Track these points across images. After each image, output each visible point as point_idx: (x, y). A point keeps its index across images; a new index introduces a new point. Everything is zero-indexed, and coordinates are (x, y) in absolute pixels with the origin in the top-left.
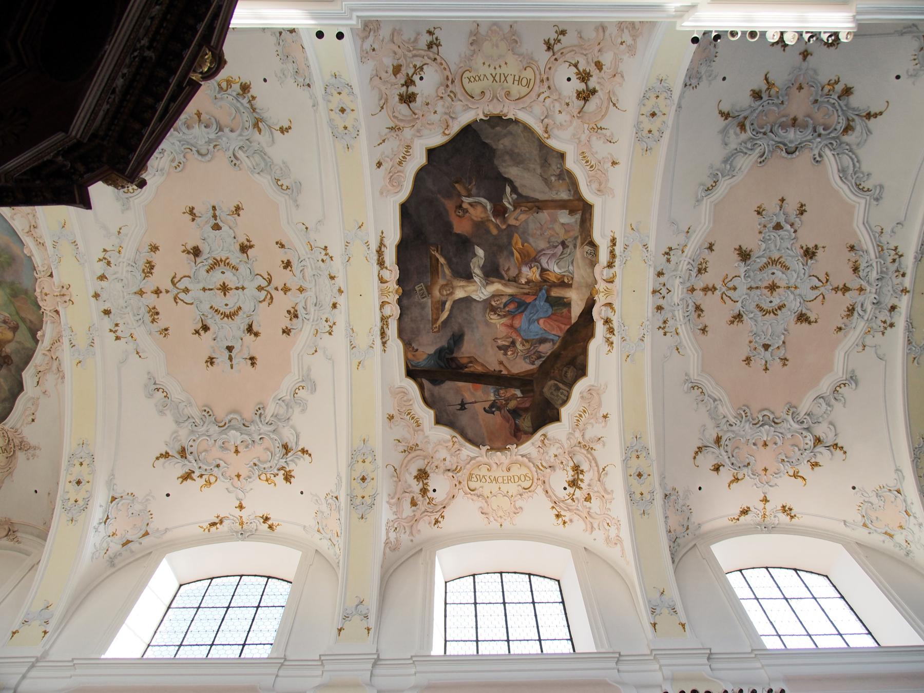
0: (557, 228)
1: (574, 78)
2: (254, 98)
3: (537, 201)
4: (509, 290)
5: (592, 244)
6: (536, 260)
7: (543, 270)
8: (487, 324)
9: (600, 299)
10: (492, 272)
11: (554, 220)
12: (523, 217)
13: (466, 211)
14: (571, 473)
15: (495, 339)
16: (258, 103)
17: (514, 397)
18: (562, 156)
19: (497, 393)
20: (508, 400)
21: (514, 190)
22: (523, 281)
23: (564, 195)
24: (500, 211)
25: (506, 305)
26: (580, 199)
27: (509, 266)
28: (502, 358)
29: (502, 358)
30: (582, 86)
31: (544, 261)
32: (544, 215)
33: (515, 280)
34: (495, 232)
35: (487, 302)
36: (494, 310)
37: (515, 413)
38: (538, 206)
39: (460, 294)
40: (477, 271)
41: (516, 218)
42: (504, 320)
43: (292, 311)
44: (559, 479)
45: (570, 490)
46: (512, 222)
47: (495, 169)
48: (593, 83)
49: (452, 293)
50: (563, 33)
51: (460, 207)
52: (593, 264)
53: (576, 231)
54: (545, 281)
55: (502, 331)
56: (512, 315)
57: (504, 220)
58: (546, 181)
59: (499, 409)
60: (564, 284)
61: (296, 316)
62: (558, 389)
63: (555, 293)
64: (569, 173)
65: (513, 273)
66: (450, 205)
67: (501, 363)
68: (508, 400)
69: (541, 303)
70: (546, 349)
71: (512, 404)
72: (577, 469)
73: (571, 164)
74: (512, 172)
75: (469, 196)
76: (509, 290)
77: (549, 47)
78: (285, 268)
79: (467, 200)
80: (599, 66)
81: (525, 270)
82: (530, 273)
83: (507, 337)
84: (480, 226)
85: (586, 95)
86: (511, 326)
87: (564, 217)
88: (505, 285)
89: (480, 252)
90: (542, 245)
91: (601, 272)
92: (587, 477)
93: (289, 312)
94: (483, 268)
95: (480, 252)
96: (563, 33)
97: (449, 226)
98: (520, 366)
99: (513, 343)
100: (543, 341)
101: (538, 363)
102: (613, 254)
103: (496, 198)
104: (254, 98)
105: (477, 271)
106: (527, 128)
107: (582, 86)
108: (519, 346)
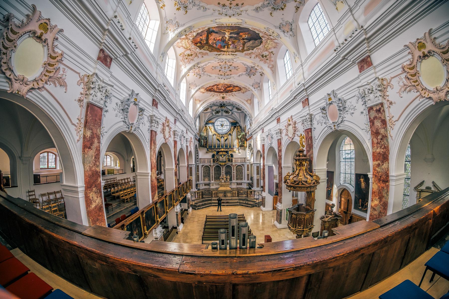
0: (239, 47)
1: (266, 55)
2: (280, 10)
3: (245, 45)
4: (227, 40)
5: (236, 52)
6: (233, 44)
7: (231, 45)
8: (219, 37)
9: (225, 53)
10: (231, 37)
11: (241, 47)
12: (242, 42)
13: (245, 35)
14: (190, 54)
15: (216, 38)
16: (278, 10)
17: (204, 42)
18: (253, 50)
19: (204, 39)
20: (203, 41)
21: (248, 42)
22: (229, 42)
23: (245, 49)
24: (243, 39)
25: (224, 39)
26: (244, 51)
27: (232, 40)
28: (212, 39)
29: (212, 39)
30: (264, 56)
31: (233, 45)
32: (242, 45)
33: (229, 40)
34: (239, 38)
35: (225, 36)
36: (223, 37)
37: (201, 43)
38: (244, 44)
39: (227, 33)
40: (231, 35)
41: (242, 41)
42: (220, 39)
43: (225, 5)
44: (188, 52)
45: (187, 55)
46: (241, 41)
47: (252, 40)
48: (265, 58)
49: (227, 32)
50: (273, 55)
51: (246, 34)
52: (232, 52)
53: (238, 49)
54: (229, 45)
55: (218, 39)
56: (221, 39)
57: (241, 40)
58: (248, 46)
59: (201, 40)
60: (228, 48)
61: (223, 6)
62: (206, 48)
63: (226, 46)
64: (249, 50)
65: (230, 40)
66: (246, 33)
67: (211, 39)
68: (203, 41)
69: (224, 44)
70: (215, 45)
71: (202, 42)
72: (192, 55)
73: (251, 51)
74: (251, 42)
75: (248, 36)
76: (227, 40)
77: (272, 52)
78: (236, 4)
79: (247, 35)
80: (267, 59)
81: (231, 42)
82: (230, 43)
83: (217, 39)
84: (241, 36)
85: (263, 56)
86: (219, 40)
87: (241, 48)
88: (228, 39)
89: (235, 36)
90: (236, 45)
91: (230, 53)
92: (190, 57)
93: (224, 4)
94: (232, 36)
95: (235, 36)
96: (273, 55)
97: (242, 32)
98: (210, 42)
99: (215, 40)
100: (216, 45)
101: (212, 44)
102: (233, 55)
103: (246, 39)
104: (280, 10)
105: (231, 35)
106: (259, 46)
107: (264, 56)
108: (214, 41)
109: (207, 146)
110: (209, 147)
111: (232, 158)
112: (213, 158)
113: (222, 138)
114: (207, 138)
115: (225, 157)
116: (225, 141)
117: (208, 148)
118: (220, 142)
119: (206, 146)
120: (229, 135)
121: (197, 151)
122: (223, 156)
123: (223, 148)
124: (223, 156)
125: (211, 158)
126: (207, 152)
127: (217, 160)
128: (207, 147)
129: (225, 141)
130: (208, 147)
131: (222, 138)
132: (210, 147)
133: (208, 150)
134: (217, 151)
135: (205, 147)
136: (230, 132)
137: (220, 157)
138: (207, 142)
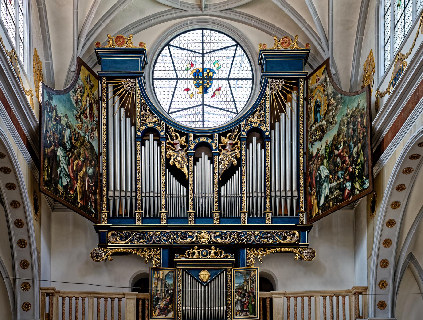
109: (98, 211)
110: (109, 219)
111: (267, 294)
112: (142, 295)
113: (204, 158)
114: (103, 159)
115: (223, 277)
116: (222, 183)
117: (104, 222)
118: (185, 182)
119: (91, 207)
120: (249, 141)
121: (22, 243)
122: (204, 275)
123: (208, 229)
124: (204, 275)
125: (127, 291)
126: (95, 256)
127: (162, 304)
128: (96, 220)
129: (222, 183)
130: (104, 217)
131: (204, 158)
132: (121, 219)
133: (104, 239)
134: (163, 248)
135: (87, 214)
136: (255, 121)
137: (187, 277)
138: (98, 184)
